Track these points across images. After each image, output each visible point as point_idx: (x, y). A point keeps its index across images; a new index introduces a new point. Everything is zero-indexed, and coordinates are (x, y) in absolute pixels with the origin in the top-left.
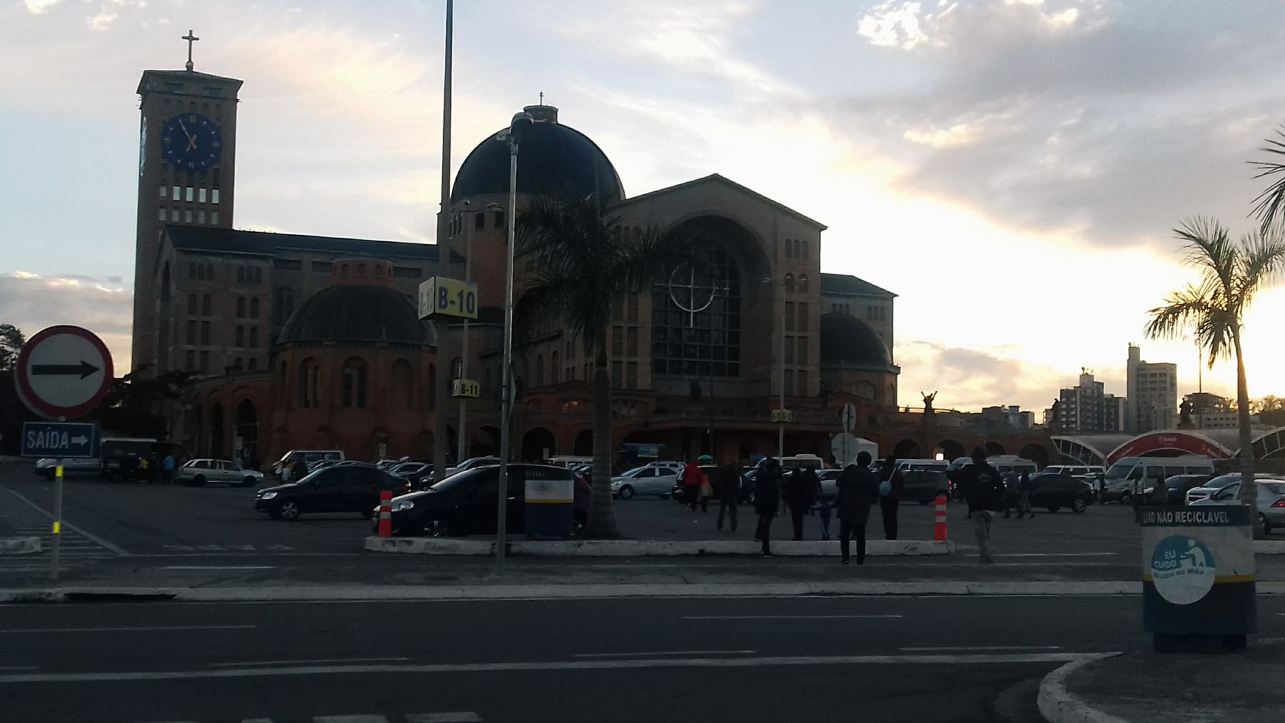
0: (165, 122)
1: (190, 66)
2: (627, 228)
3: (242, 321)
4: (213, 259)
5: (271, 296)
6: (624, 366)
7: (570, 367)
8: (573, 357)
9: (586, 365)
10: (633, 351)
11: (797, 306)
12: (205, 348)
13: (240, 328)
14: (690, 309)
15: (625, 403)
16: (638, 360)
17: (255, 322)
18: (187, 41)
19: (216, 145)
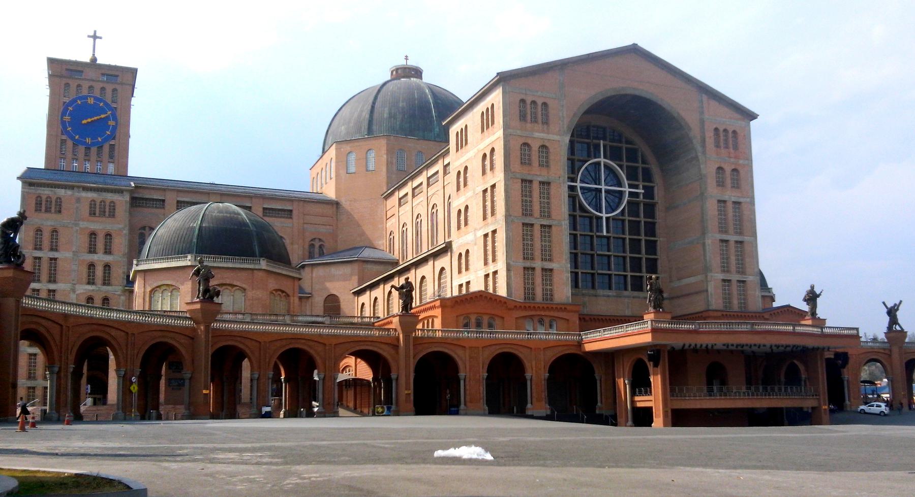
0: (64, 103)
1: (94, 60)
2: (534, 102)
3: (94, 257)
4: (61, 192)
5: (126, 232)
6: (538, 273)
7: (464, 282)
8: (467, 269)
9: (487, 276)
10: (547, 256)
12: (52, 286)
13: (91, 266)
14: (601, 212)
15: (541, 322)
17: (108, 258)
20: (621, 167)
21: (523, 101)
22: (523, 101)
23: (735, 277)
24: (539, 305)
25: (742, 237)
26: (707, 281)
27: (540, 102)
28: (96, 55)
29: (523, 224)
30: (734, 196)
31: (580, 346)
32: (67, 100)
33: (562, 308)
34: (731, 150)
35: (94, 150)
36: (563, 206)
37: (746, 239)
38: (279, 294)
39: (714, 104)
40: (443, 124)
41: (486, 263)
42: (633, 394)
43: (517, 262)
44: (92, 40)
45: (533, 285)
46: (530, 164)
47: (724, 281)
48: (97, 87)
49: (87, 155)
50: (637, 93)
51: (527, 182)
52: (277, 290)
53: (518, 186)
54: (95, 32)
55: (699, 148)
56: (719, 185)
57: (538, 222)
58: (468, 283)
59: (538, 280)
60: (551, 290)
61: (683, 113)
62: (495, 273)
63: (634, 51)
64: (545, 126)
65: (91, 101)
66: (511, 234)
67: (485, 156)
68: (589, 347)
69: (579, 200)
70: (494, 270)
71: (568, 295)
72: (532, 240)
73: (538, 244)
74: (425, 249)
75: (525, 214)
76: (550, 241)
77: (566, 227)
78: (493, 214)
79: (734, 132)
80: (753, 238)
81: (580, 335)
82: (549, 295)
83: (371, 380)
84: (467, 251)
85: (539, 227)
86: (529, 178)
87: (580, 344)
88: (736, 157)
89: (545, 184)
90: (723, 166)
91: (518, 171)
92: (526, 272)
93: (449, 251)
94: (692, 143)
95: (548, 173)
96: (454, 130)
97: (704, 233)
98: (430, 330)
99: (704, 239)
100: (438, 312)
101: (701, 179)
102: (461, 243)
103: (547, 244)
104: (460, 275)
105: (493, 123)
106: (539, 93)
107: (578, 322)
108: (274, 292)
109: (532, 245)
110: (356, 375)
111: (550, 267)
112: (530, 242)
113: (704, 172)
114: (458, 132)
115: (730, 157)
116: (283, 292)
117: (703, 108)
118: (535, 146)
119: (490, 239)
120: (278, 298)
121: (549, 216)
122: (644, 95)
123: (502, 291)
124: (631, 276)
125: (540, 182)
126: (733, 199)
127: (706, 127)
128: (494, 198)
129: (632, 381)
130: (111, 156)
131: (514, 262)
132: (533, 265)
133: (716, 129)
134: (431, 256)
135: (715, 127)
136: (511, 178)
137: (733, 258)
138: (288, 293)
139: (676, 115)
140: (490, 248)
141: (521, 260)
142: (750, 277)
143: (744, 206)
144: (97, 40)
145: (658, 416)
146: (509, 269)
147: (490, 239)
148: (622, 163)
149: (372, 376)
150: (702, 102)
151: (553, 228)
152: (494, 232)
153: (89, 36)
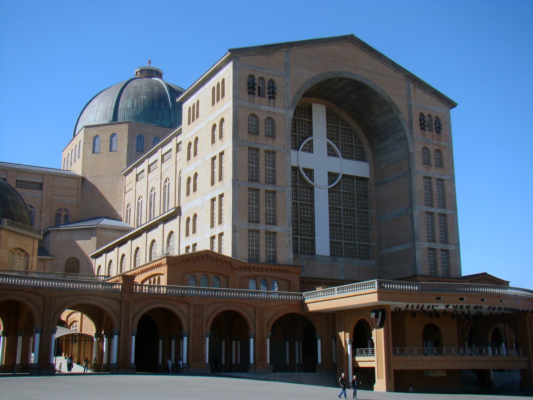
8: (194, 232)
9: (213, 238)
11: (434, 181)
20: (337, 145)
21: (252, 77)
22: (252, 77)
23: (439, 246)
24: (263, 266)
25: (444, 210)
26: (415, 249)
27: (267, 79)
29: (249, 189)
30: (437, 174)
31: (303, 305)
33: (285, 269)
34: (435, 132)
36: (287, 173)
37: (448, 212)
38: (19, 253)
39: (419, 92)
40: (177, 100)
41: (212, 226)
42: (354, 354)
43: (242, 224)
45: (257, 247)
46: (257, 133)
47: (429, 249)
50: (354, 78)
51: (254, 151)
52: (16, 249)
53: (245, 153)
55: (407, 129)
56: (424, 164)
57: (263, 187)
58: (195, 245)
59: (262, 243)
60: (275, 253)
61: (393, 98)
62: (221, 234)
63: (351, 39)
64: (272, 100)
66: (237, 198)
67: (214, 126)
68: (312, 308)
69: (299, 173)
70: (220, 232)
71: (290, 258)
72: (257, 204)
73: (263, 209)
74: (157, 214)
76: (275, 206)
77: (289, 193)
78: (220, 179)
79: (437, 118)
80: (452, 211)
81: (302, 295)
82: (272, 259)
83: (94, 336)
84: (195, 216)
85: (264, 193)
86: (256, 146)
87: (303, 305)
88: (439, 139)
89: (272, 153)
90: (427, 146)
91: (247, 140)
92: (251, 234)
93: (178, 217)
94: (401, 124)
95: (273, 143)
96: (186, 106)
97: (411, 205)
98: (156, 286)
99: (412, 211)
100: (164, 270)
101: (410, 156)
102: (190, 208)
103: (271, 208)
104: (188, 237)
105: (223, 96)
106: (266, 71)
107: (298, 283)
108: (13, 251)
110: (81, 331)
111: (274, 231)
112: (255, 206)
113: (411, 150)
114: (190, 107)
115: (433, 139)
116: (23, 251)
117: (410, 94)
118: (262, 118)
119: (216, 203)
120: (17, 256)
121: (274, 183)
122: (359, 79)
123: (227, 251)
124: (345, 243)
125: (266, 151)
127: (413, 112)
128: (222, 164)
129: (353, 341)
131: (239, 224)
132: (258, 228)
133: (422, 115)
134: (162, 221)
135: (420, 112)
136: (239, 145)
137: (437, 229)
138: (27, 252)
139: (387, 99)
140: (216, 211)
141: (247, 223)
142: (451, 246)
143: (446, 183)
145: (380, 377)
146: (234, 231)
147: (216, 203)
148: (337, 141)
149: (95, 332)
150: (410, 91)
151: (277, 193)
152: (221, 196)
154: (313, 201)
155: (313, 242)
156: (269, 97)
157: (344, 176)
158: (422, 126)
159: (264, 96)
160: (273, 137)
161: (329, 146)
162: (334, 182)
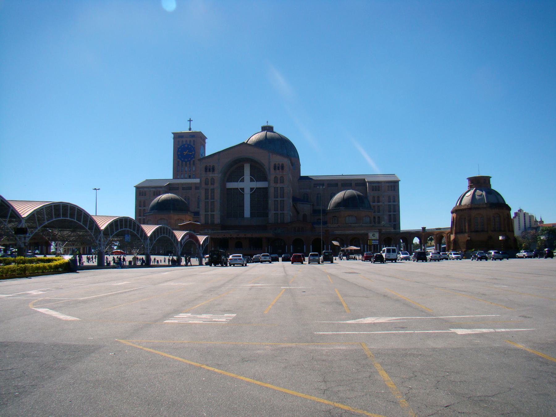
1: (190, 129)
2: (210, 166)
4: (146, 189)
6: (210, 216)
16: (214, 213)
18: (189, 122)
19: (193, 153)
22: (207, 166)
23: (279, 212)
28: (191, 127)
29: (205, 202)
32: (179, 147)
34: (281, 170)
35: (188, 163)
37: (285, 199)
44: (189, 122)
47: (275, 214)
48: (188, 140)
49: (186, 165)
51: (207, 190)
52: (178, 219)
54: (190, 119)
56: (274, 183)
64: (213, 172)
65: (186, 146)
75: (206, 199)
109: (208, 208)
111: (213, 214)
116: (181, 219)
121: (214, 199)
125: (211, 189)
126: (281, 187)
130: (194, 164)
144: (191, 122)
153: (188, 121)
154: (244, 199)
155: (244, 213)
156: (213, 172)
157: (257, 188)
158: (275, 169)
159: (211, 172)
160: (214, 184)
161: (251, 178)
162: (252, 191)
